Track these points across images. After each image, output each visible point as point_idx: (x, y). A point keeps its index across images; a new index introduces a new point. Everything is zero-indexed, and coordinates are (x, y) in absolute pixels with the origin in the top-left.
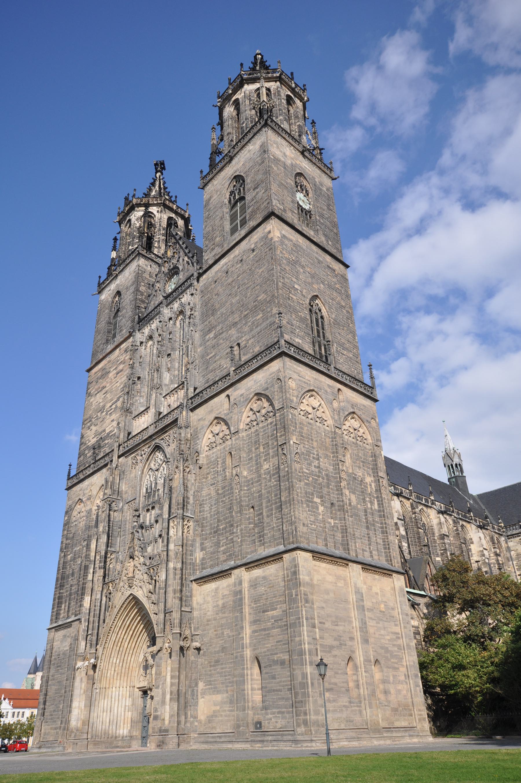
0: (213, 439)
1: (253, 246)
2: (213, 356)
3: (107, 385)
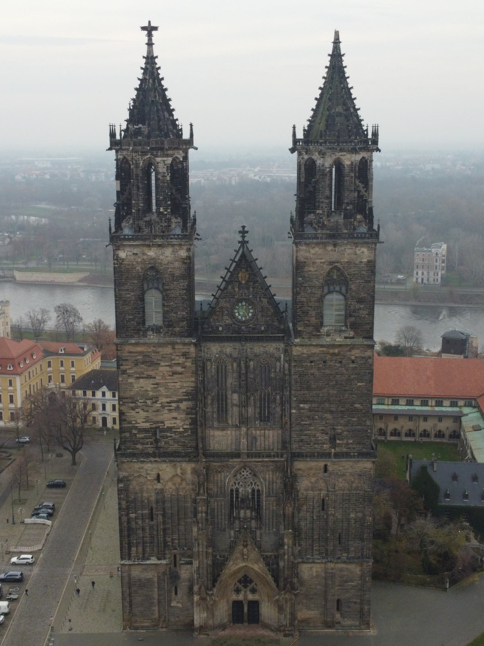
1: (353, 358)
2: (308, 424)
3: (157, 378)
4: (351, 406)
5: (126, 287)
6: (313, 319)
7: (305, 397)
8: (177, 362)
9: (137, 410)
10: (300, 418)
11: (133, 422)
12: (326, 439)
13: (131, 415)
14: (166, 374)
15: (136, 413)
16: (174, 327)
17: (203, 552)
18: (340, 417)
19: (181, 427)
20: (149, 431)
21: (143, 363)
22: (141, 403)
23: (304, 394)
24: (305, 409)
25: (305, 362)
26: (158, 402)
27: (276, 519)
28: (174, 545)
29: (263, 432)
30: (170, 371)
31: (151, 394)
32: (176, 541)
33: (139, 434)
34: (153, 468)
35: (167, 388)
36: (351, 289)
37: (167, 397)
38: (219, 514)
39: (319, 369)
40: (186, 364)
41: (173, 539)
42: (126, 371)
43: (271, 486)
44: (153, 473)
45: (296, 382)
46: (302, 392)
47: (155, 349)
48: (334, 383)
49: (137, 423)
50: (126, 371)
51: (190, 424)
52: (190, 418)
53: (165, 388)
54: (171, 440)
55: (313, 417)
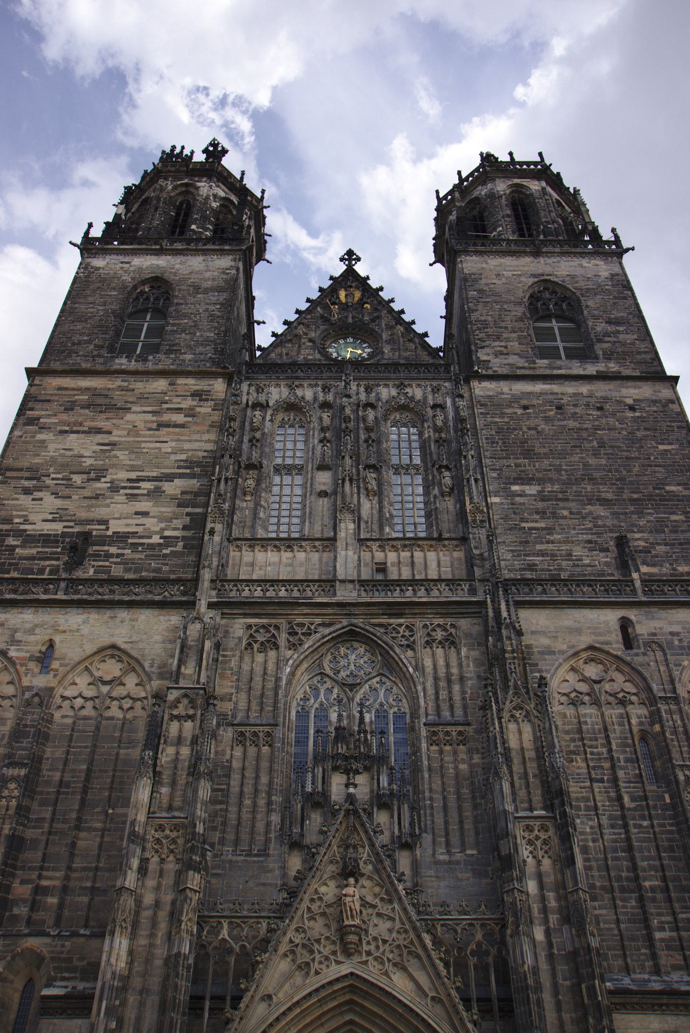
0: (583, 687)
1: (629, 401)
2: (543, 529)
3: (115, 432)
4: (654, 488)
5: (91, 299)
6: (516, 344)
7: (524, 471)
8: (177, 406)
9: (37, 495)
10: (515, 513)
11: (16, 520)
12: (607, 564)
13: (13, 505)
14: (142, 426)
15: (33, 500)
16: (181, 354)
17: (157, 904)
18: (633, 513)
19: (156, 533)
20: (58, 541)
21: (88, 406)
22: (53, 479)
23: (516, 465)
24: (526, 495)
25: (510, 406)
26: (103, 480)
27: (475, 806)
28: (36, 916)
29: (405, 554)
30: (153, 422)
31: (89, 462)
32: (53, 900)
33: (22, 546)
34: (36, 626)
35: (134, 450)
36: (587, 306)
37: (132, 469)
38: (248, 789)
39: (547, 419)
40: (198, 409)
41: (39, 890)
42: (38, 419)
43: (443, 694)
44: (32, 638)
45: (493, 443)
46: (512, 462)
47: (126, 384)
48: (595, 443)
49: (26, 521)
50: (38, 419)
51: (185, 528)
52: (188, 514)
53: (132, 452)
54: (116, 563)
55: (554, 513)
